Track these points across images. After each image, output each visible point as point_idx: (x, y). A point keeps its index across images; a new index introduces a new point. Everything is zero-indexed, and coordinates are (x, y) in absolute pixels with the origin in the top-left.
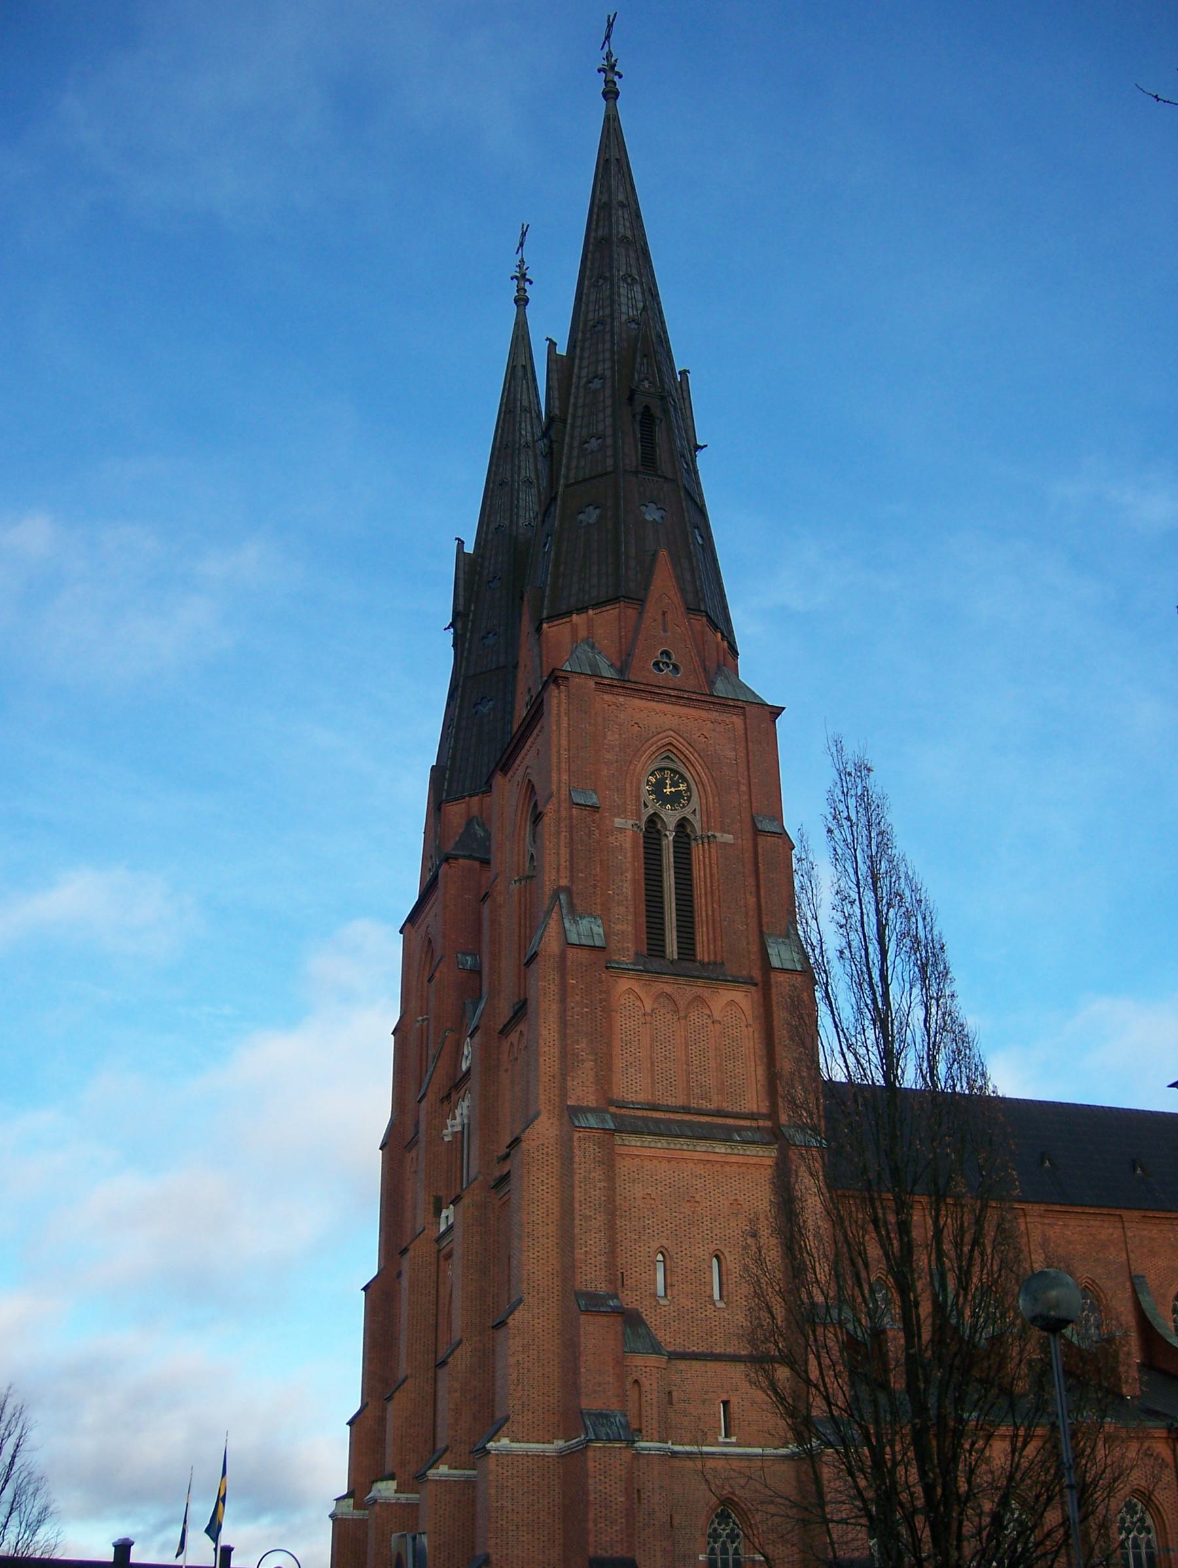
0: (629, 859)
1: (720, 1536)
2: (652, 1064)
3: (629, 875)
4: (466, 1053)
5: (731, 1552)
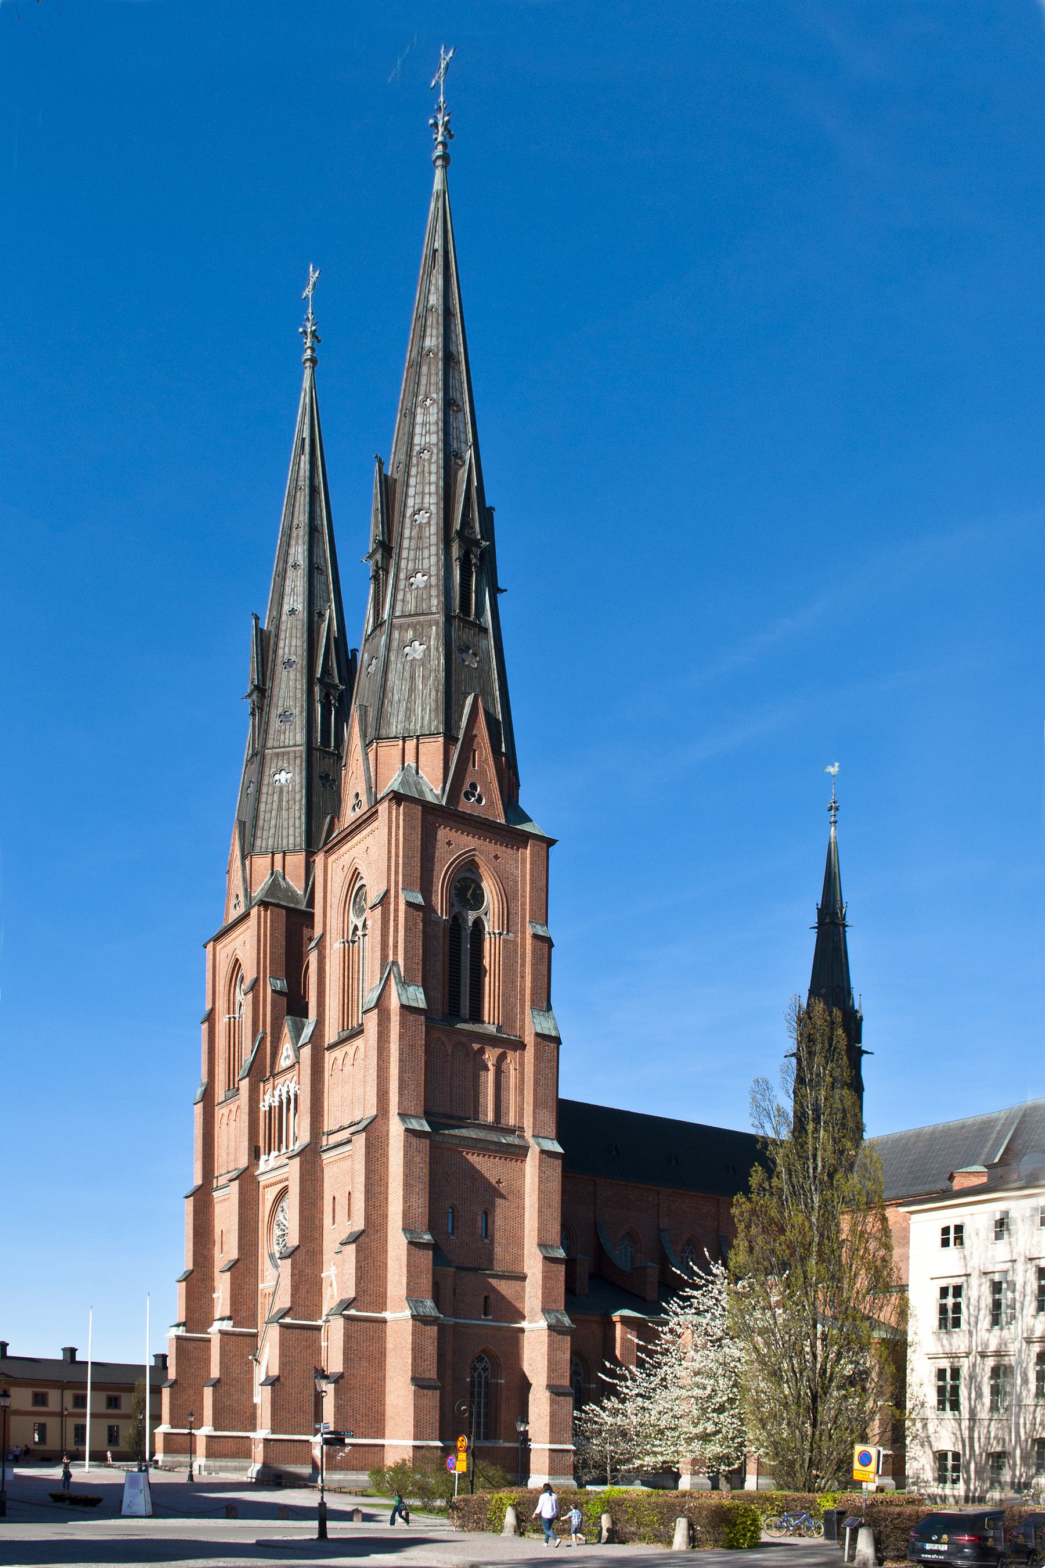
0: (441, 945)
1: (478, 1369)
2: (451, 1089)
3: (441, 957)
4: (285, 1054)
5: (483, 1377)
